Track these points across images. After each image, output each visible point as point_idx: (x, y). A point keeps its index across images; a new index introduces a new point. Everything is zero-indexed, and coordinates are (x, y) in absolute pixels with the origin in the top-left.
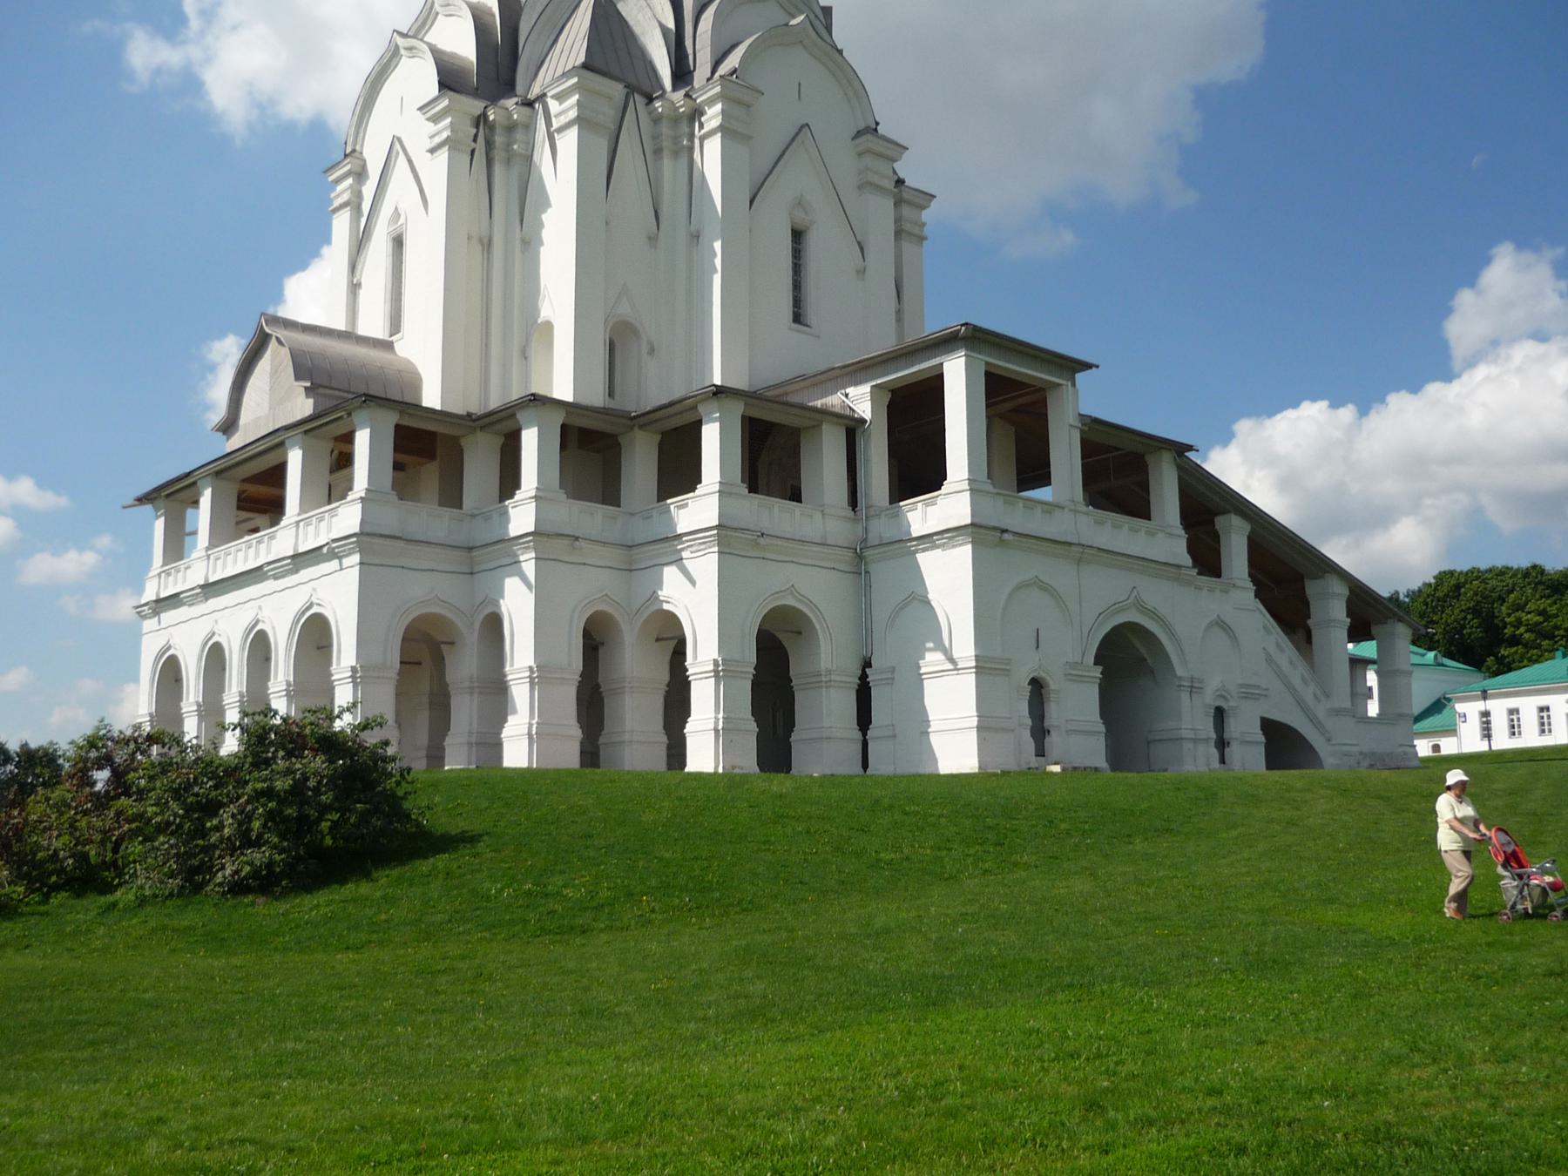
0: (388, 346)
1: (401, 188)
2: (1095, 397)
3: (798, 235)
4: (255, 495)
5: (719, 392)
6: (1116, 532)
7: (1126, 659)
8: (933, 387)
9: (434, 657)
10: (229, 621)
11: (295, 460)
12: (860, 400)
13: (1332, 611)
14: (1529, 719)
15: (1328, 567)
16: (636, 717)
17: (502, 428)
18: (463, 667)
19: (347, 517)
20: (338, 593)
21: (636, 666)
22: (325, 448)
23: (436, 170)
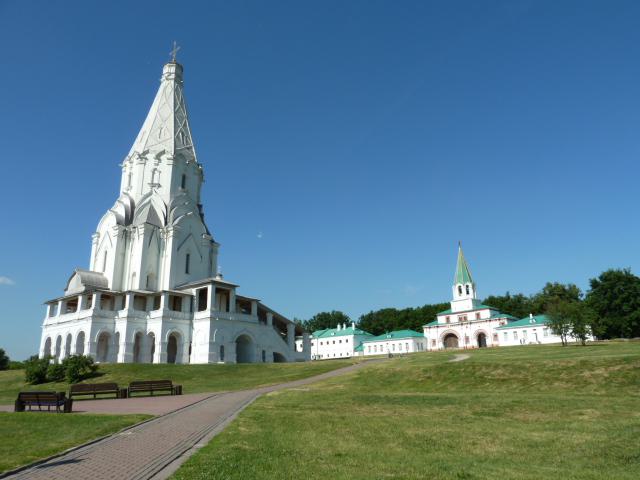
0: (102, 274)
1: (107, 242)
2: (239, 292)
3: (188, 256)
4: (71, 304)
5: (165, 292)
6: (246, 317)
7: (242, 343)
8: (206, 290)
9: (106, 341)
10: (64, 332)
11: (80, 298)
12: (194, 292)
13: (291, 329)
14: (379, 347)
15: (290, 322)
16: (145, 350)
17: (123, 295)
18: (111, 342)
19: (90, 312)
20: (87, 327)
21: (145, 342)
22: (87, 297)
23: (115, 240)
